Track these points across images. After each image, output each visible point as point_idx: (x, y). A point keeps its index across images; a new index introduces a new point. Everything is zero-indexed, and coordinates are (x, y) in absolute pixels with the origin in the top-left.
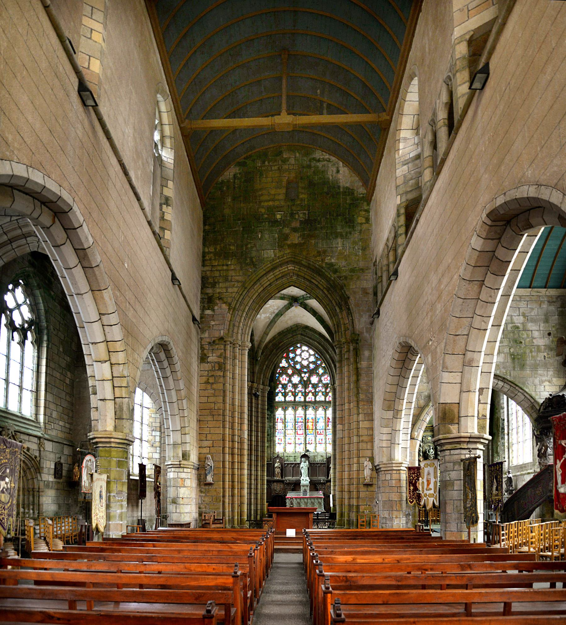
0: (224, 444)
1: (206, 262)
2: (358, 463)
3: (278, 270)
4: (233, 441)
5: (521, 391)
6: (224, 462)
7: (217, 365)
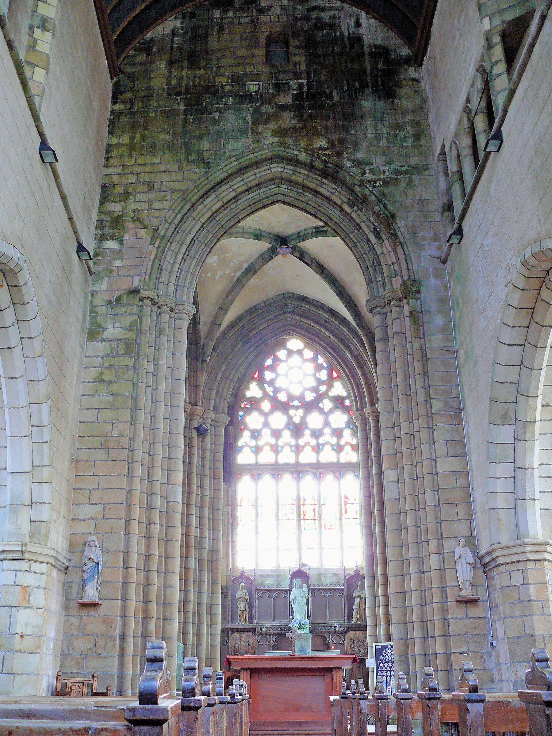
0: (129, 511)
1: (111, 161)
2: (440, 552)
3: (252, 173)
4: (150, 508)
6: (127, 553)
7: (122, 346)
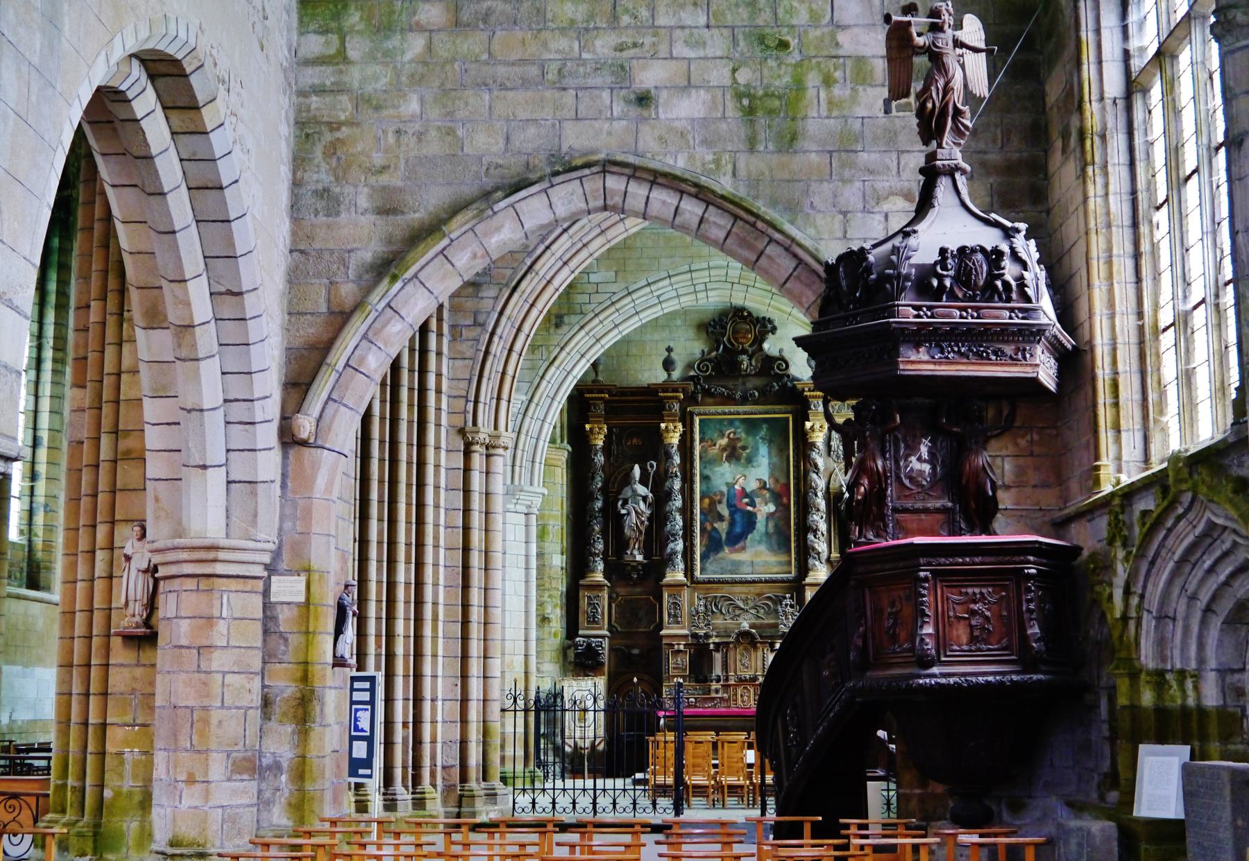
5: (777, 236)
